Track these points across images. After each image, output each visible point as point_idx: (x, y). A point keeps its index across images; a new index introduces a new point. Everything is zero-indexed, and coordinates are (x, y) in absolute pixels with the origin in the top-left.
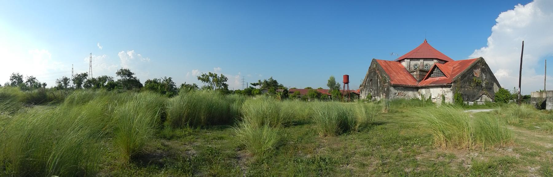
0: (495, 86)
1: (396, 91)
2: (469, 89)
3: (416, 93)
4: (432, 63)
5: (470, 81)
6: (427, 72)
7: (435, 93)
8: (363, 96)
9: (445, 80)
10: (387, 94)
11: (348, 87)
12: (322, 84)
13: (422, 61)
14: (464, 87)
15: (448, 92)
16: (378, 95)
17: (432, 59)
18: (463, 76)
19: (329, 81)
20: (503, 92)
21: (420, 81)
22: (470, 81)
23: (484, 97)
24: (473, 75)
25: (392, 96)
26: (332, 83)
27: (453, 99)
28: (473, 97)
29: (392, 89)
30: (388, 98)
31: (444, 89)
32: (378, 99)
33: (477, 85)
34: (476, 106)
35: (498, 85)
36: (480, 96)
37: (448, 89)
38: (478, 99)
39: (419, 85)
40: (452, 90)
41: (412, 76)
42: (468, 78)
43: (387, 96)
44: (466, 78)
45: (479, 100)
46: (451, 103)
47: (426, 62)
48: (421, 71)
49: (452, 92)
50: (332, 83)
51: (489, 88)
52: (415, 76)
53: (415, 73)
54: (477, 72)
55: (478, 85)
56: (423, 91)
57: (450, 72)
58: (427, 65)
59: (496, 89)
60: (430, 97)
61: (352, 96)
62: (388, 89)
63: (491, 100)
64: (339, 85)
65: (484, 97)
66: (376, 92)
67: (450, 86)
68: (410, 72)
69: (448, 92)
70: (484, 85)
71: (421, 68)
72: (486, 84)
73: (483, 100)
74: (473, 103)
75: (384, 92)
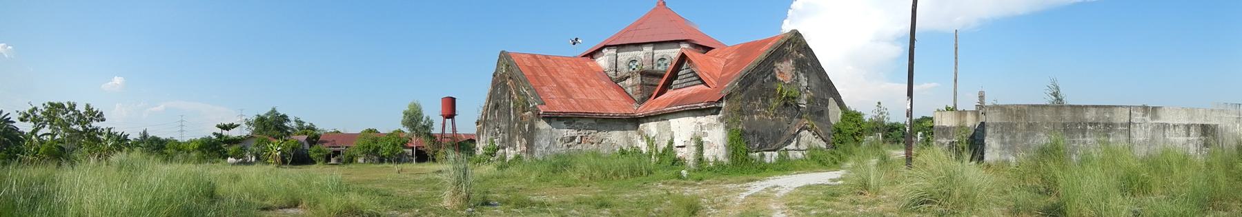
0: (832, 103)
1: (573, 133)
2: (763, 116)
3: (631, 133)
4: (673, 53)
5: (767, 93)
6: (661, 76)
7: (682, 130)
8: (480, 147)
9: (701, 93)
10: (531, 137)
11: (453, 123)
12: (390, 122)
13: (648, 49)
14: (751, 113)
15: (710, 126)
16: (510, 143)
17: (678, 42)
18: (747, 81)
19: (406, 113)
20: (852, 117)
21: (643, 101)
22: (767, 93)
23: (806, 136)
24: (774, 79)
25: (542, 144)
26: (413, 118)
27: (727, 148)
28: (774, 139)
29: (542, 125)
30: (532, 153)
31: (704, 120)
32: (510, 154)
33: (786, 105)
34: (785, 166)
35: (840, 103)
36: (795, 135)
37: (712, 119)
38: (790, 142)
39: (641, 111)
40: (721, 120)
41: (623, 90)
42: (762, 87)
43: (530, 146)
44: (754, 87)
45: (792, 146)
46: (721, 157)
47: (659, 53)
48: (644, 74)
49: (722, 126)
50: (413, 118)
51: (819, 113)
52: (629, 90)
53: (629, 82)
54: (785, 70)
55: (789, 103)
56: (652, 128)
57: (718, 73)
58: (662, 59)
59: (835, 115)
60: (671, 143)
61: (465, 146)
62: (532, 127)
63: (823, 145)
64: (431, 123)
65: (806, 136)
66: (506, 136)
67: (716, 111)
68: (617, 81)
69: (710, 126)
70: (803, 103)
71: (647, 67)
72: (809, 102)
73: (803, 146)
74: (776, 154)
75: (524, 135)
